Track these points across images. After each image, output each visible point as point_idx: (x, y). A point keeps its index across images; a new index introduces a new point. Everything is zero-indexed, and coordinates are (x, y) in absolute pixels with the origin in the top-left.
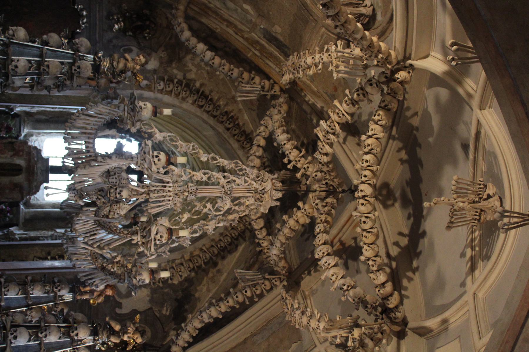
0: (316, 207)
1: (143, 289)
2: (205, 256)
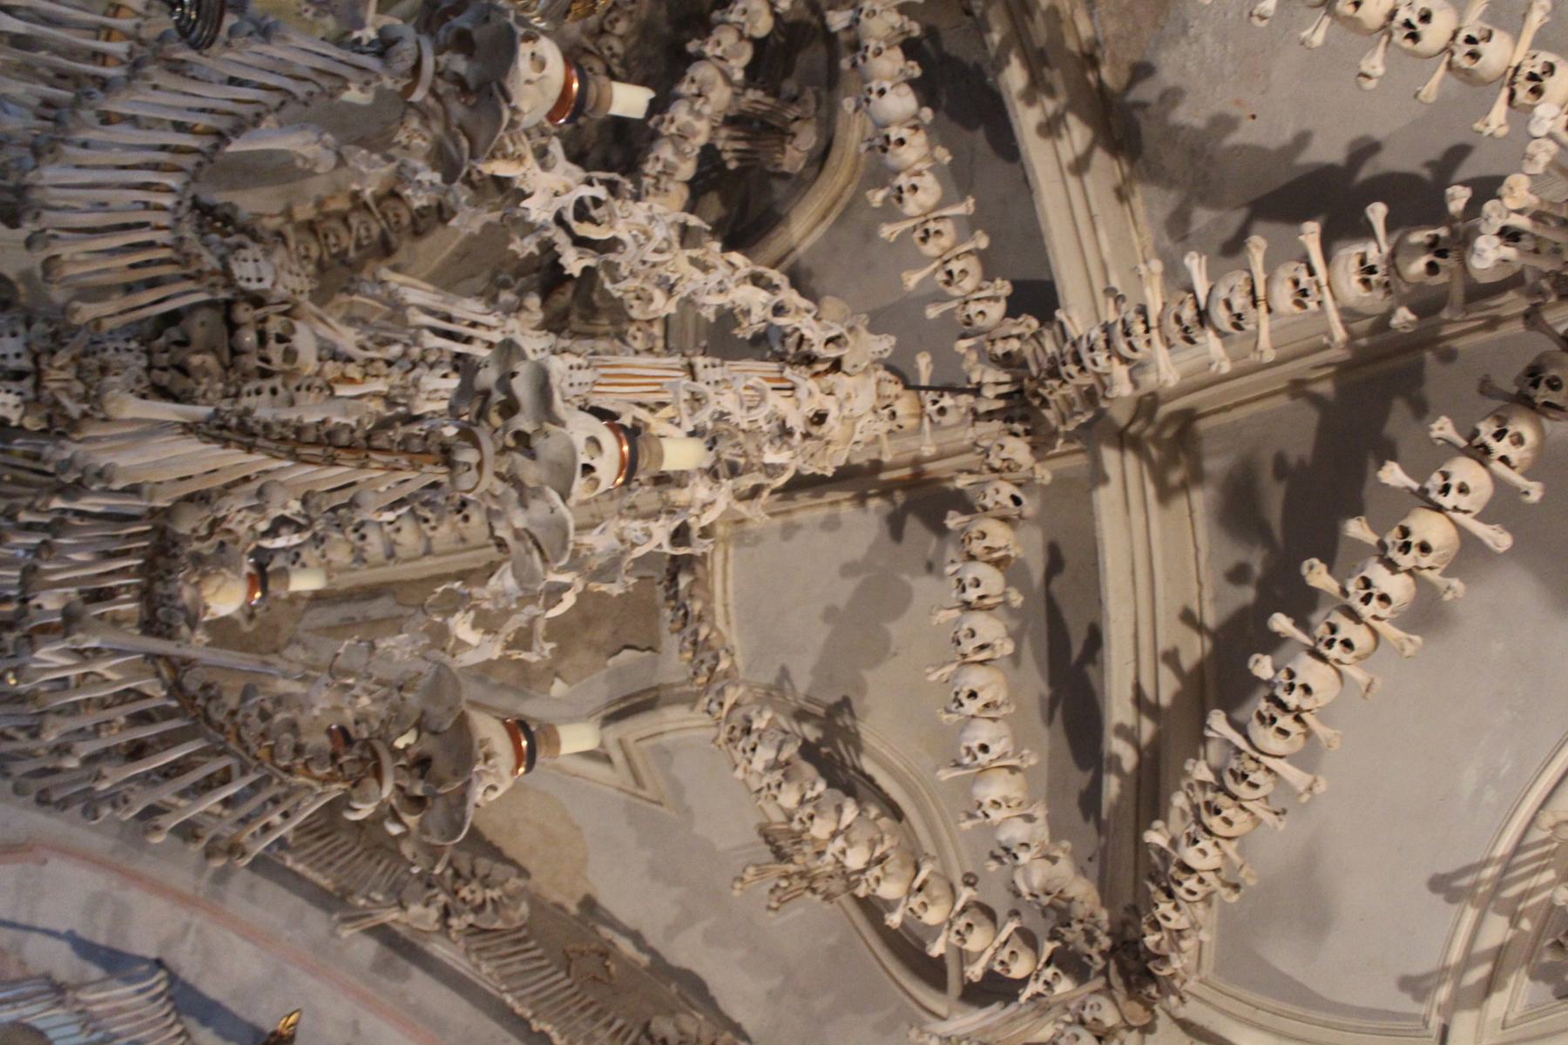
0: (936, 418)
2: (368, 229)
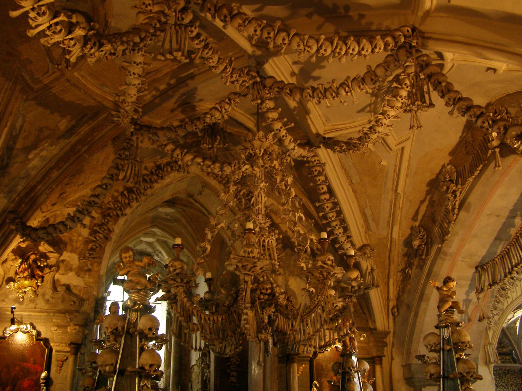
1: (289, 283)
